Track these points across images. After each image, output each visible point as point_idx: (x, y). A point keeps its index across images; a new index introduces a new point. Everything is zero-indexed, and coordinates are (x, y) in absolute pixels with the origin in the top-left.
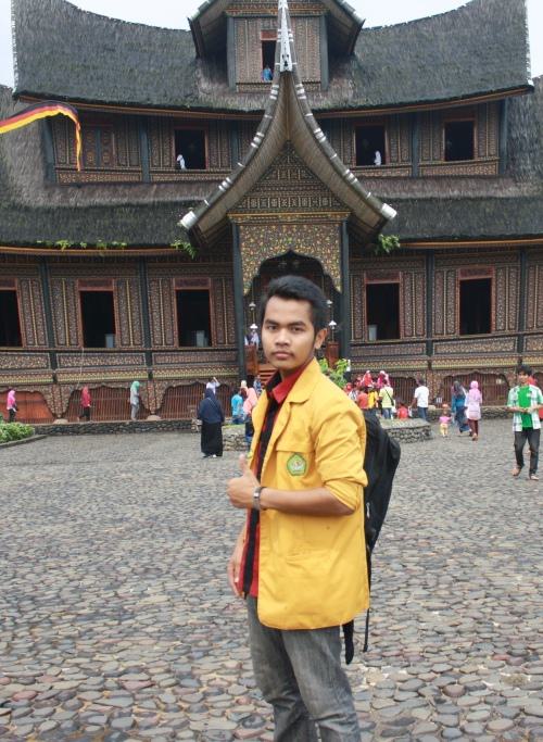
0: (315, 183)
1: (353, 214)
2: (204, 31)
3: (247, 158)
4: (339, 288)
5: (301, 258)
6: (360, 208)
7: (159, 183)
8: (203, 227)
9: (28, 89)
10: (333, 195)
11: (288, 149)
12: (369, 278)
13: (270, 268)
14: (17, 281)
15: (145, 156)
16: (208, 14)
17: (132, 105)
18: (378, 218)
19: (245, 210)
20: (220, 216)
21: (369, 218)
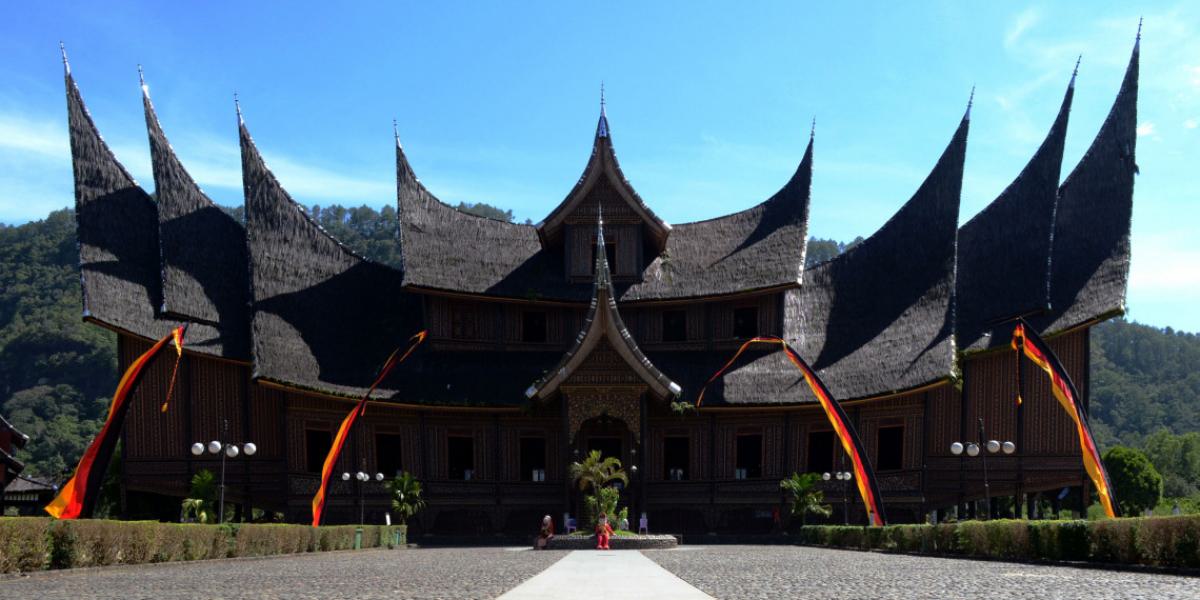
2: (548, 235)
6: (654, 384)
8: (541, 395)
9: (414, 283)
10: (637, 374)
11: (604, 344)
13: (590, 425)
18: (667, 393)
21: (661, 390)
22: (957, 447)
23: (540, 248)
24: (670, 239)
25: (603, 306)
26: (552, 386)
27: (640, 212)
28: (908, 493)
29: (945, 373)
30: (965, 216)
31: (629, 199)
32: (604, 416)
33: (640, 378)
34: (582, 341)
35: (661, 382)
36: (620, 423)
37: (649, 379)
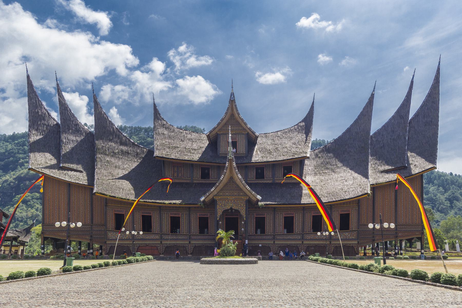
1: (249, 198)
3: (224, 174)
6: (251, 196)
7: (196, 183)
11: (231, 179)
14: (152, 213)
16: (212, 133)
19: (219, 196)
21: (253, 199)
22: (371, 226)
23: (208, 143)
24: (259, 139)
25: (231, 165)
26: (211, 197)
28: (352, 240)
29: (366, 192)
30: (373, 130)
32: (231, 209)
36: (237, 212)
37: (248, 193)
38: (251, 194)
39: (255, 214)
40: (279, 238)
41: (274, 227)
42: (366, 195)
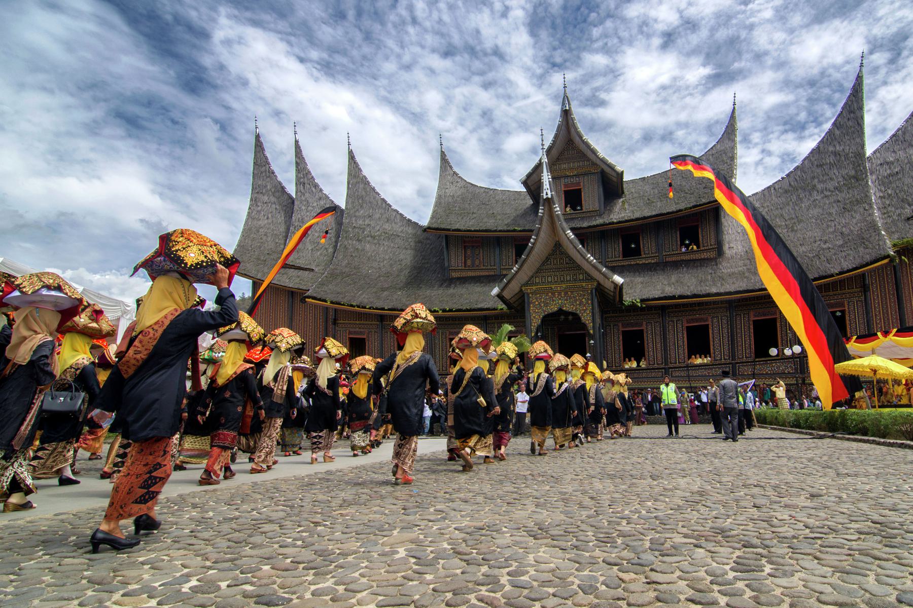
0: (574, 266)
1: (599, 284)
4: (591, 332)
5: (567, 313)
10: (586, 273)
11: (558, 248)
12: (623, 326)
15: (497, 261)
16: (532, 178)
17: (486, 231)
19: (532, 284)
20: (517, 290)
21: (608, 285)
27: (598, 162)
31: (589, 154)
33: (589, 275)
34: (533, 244)
35: (604, 275)
36: (576, 317)
38: (600, 271)
39: (620, 325)
40: (677, 374)
41: (665, 350)
42: (886, 261)
